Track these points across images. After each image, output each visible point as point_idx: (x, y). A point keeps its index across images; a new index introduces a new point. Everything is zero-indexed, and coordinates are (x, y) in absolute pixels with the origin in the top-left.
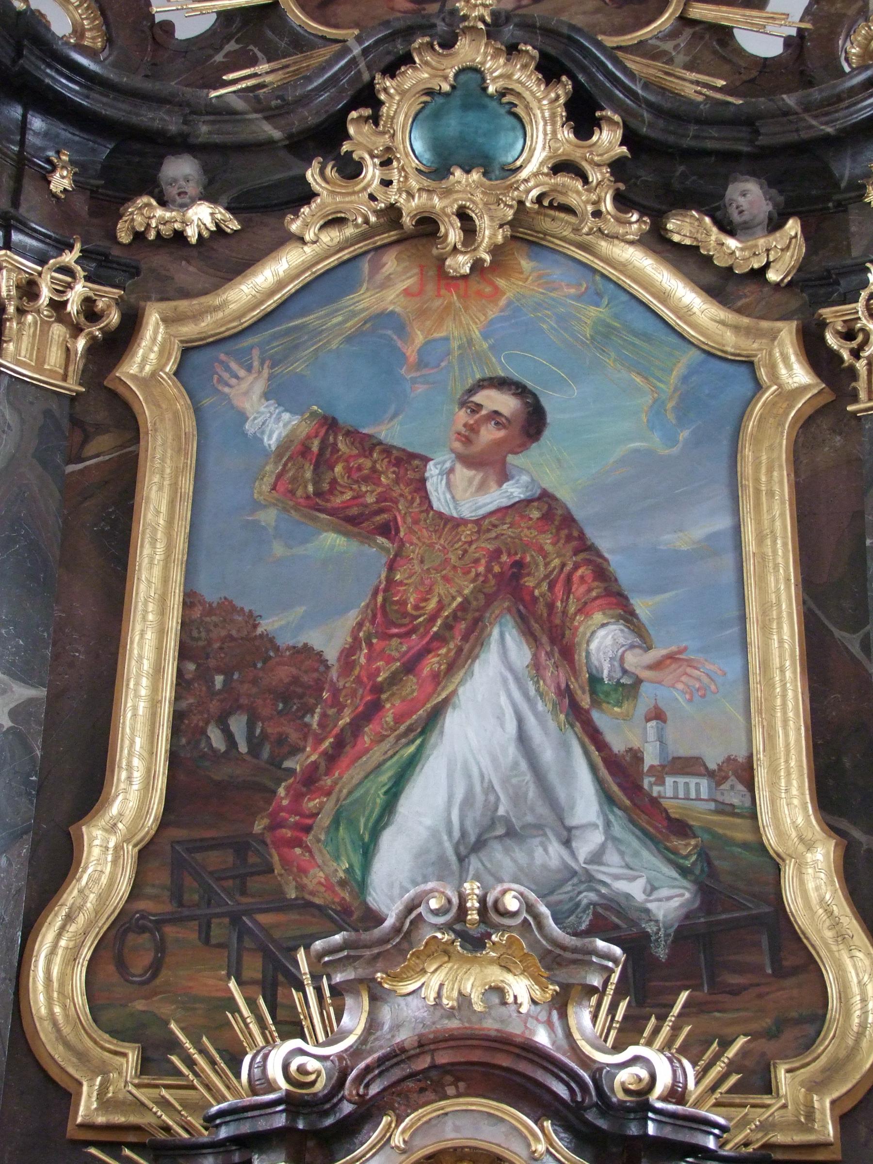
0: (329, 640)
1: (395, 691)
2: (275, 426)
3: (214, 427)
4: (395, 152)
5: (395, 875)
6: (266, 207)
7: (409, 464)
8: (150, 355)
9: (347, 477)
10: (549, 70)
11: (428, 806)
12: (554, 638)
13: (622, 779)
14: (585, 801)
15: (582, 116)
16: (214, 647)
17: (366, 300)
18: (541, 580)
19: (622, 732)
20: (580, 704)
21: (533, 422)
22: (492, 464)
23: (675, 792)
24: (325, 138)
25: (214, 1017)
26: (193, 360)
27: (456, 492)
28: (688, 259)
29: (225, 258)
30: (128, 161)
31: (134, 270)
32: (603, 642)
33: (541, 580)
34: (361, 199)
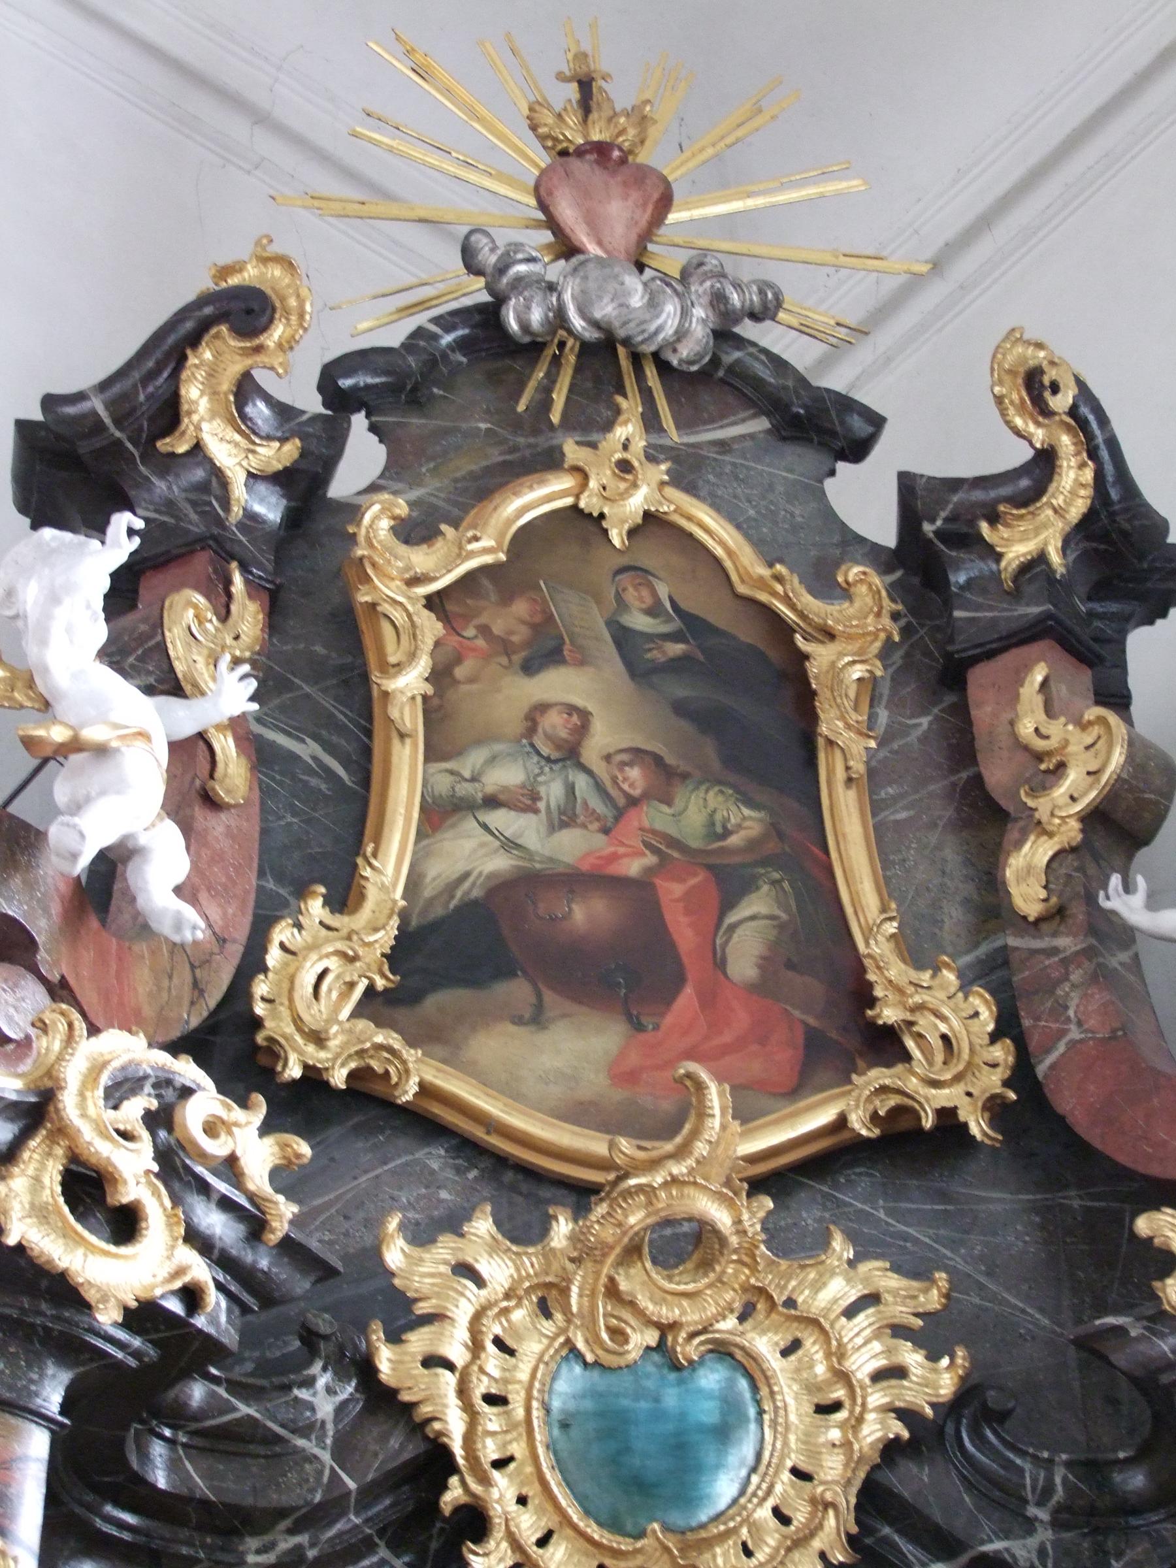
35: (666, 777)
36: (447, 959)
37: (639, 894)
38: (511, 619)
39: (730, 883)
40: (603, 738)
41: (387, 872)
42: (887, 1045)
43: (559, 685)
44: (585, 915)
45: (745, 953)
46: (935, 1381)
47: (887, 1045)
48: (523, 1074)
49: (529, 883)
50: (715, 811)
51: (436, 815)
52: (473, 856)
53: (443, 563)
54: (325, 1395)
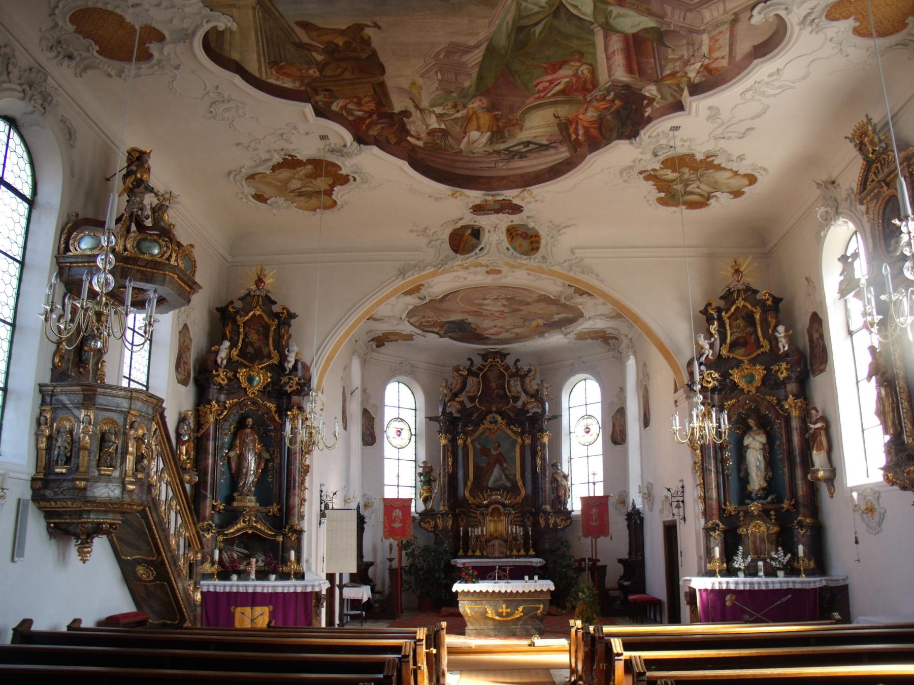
0: (484, 465)
1: (490, 471)
2: (479, 447)
3: (475, 448)
4: (487, 424)
5: (490, 484)
6: (477, 425)
7: (490, 450)
8: (469, 441)
9: (485, 451)
10: (500, 415)
11: (492, 479)
12: (501, 465)
13: (506, 476)
14: (504, 478)
15: (503, 419)
16: (476, 467)
17: (486, 435)
18: (500, 460)
19: (507, 472)
20: (503, 470)
21: (499, 446)
22: (496, 450)
23: (511, 477)
24: (482, 420)
25: (478, 496)
26: (472, 442)
27: (494, 452)
28: (511, 430)
29: (474, 431)
30: (465, 425)
31: (466, 434)
32: (505, 465)
33: (500, 460)
34: (485, 426)
35: (746, 327)
36: (733, 346)
37: (745, 338)
38: (734, 317)
39: (751, 335)
40: (742, 325)
41: (728, 341)
42: (762, 346)
43: (738, 322)
44: (741, 340)
45: (752, 340)
46: (765, 372)
47: (762, 346)
48: (739, 354)
49: (737, 339)
50: (750, 329)
51: (731, 334)
52: (734, 337)
53: (728, 315)
54: (728, 381)
